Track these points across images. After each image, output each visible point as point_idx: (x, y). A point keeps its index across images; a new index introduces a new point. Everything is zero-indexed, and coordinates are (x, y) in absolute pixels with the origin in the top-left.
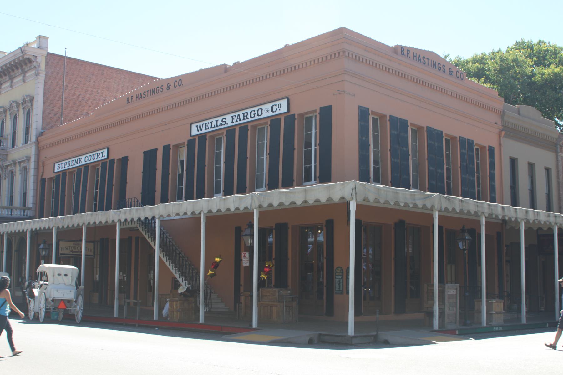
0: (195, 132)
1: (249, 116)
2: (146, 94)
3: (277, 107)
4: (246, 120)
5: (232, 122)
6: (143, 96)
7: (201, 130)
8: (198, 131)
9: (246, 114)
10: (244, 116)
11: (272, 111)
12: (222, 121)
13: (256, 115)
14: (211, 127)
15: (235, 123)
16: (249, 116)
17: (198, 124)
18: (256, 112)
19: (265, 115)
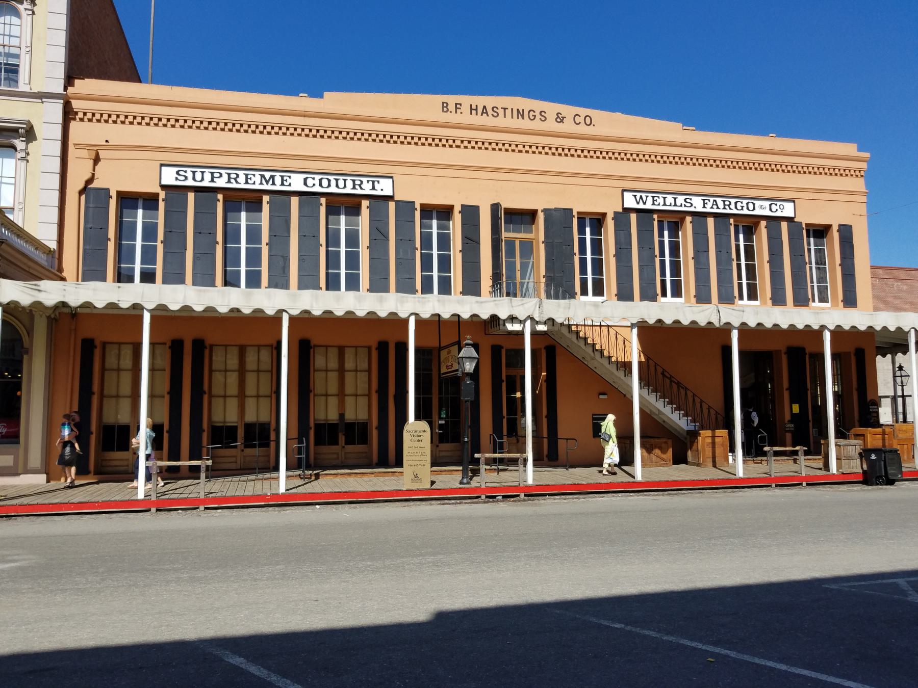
0: (630, 202)
1: (733, 206)
3: (778, 207)
4: (728, 211)
5: (704, 207)
7: (644, 203)
8: (638, 203)
9: (727, 203)
10: (725, 205)
11: (771, 210)
12: (685, 200)
13: (745, 208)
14: (665, 204)
15: (708, 210)
16: (733, 206)
17: (638, 195)
18: (744, 204)
19: (758, 212)
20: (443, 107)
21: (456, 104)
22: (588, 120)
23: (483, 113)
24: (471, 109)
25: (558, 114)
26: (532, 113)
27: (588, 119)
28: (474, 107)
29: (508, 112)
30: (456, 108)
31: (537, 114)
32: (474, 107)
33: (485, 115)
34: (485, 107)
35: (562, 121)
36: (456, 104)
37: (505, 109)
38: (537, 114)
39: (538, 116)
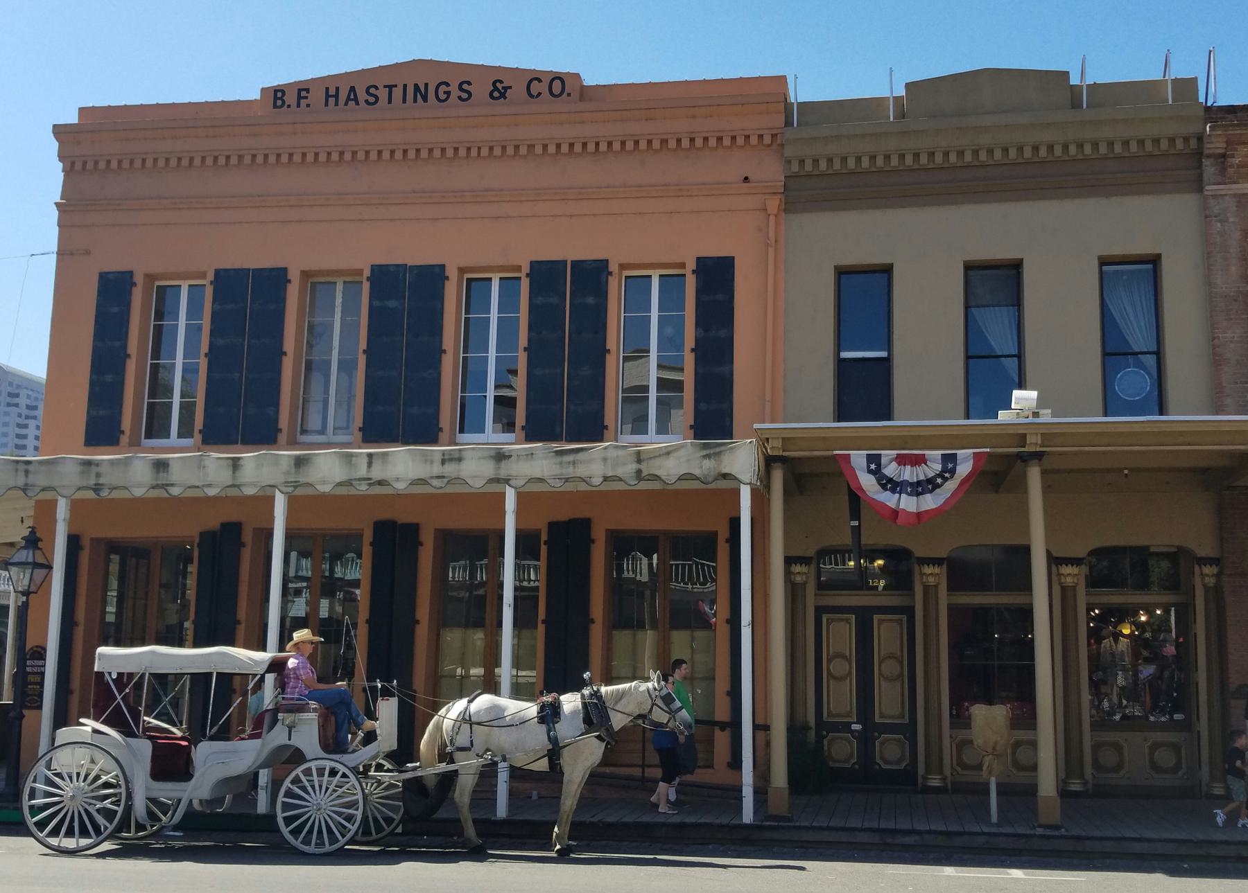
2: (383, 94)
6: (362, 96)
20: (276, 98)
21: (300, 91)
23: (348, 99)
24: (328, 96)
25: (494, 83)
26: (443, 88)
27: (557, 84)
29: (397, 93)
30: (300, 97)
31: (454, 89)
32: (332, 92)
33: (352, 103)
34: (352, 89)
35: (503, 96)
36: (300, 91)
37: (390, 87)
38: (454, 89)
39: (455, 92)
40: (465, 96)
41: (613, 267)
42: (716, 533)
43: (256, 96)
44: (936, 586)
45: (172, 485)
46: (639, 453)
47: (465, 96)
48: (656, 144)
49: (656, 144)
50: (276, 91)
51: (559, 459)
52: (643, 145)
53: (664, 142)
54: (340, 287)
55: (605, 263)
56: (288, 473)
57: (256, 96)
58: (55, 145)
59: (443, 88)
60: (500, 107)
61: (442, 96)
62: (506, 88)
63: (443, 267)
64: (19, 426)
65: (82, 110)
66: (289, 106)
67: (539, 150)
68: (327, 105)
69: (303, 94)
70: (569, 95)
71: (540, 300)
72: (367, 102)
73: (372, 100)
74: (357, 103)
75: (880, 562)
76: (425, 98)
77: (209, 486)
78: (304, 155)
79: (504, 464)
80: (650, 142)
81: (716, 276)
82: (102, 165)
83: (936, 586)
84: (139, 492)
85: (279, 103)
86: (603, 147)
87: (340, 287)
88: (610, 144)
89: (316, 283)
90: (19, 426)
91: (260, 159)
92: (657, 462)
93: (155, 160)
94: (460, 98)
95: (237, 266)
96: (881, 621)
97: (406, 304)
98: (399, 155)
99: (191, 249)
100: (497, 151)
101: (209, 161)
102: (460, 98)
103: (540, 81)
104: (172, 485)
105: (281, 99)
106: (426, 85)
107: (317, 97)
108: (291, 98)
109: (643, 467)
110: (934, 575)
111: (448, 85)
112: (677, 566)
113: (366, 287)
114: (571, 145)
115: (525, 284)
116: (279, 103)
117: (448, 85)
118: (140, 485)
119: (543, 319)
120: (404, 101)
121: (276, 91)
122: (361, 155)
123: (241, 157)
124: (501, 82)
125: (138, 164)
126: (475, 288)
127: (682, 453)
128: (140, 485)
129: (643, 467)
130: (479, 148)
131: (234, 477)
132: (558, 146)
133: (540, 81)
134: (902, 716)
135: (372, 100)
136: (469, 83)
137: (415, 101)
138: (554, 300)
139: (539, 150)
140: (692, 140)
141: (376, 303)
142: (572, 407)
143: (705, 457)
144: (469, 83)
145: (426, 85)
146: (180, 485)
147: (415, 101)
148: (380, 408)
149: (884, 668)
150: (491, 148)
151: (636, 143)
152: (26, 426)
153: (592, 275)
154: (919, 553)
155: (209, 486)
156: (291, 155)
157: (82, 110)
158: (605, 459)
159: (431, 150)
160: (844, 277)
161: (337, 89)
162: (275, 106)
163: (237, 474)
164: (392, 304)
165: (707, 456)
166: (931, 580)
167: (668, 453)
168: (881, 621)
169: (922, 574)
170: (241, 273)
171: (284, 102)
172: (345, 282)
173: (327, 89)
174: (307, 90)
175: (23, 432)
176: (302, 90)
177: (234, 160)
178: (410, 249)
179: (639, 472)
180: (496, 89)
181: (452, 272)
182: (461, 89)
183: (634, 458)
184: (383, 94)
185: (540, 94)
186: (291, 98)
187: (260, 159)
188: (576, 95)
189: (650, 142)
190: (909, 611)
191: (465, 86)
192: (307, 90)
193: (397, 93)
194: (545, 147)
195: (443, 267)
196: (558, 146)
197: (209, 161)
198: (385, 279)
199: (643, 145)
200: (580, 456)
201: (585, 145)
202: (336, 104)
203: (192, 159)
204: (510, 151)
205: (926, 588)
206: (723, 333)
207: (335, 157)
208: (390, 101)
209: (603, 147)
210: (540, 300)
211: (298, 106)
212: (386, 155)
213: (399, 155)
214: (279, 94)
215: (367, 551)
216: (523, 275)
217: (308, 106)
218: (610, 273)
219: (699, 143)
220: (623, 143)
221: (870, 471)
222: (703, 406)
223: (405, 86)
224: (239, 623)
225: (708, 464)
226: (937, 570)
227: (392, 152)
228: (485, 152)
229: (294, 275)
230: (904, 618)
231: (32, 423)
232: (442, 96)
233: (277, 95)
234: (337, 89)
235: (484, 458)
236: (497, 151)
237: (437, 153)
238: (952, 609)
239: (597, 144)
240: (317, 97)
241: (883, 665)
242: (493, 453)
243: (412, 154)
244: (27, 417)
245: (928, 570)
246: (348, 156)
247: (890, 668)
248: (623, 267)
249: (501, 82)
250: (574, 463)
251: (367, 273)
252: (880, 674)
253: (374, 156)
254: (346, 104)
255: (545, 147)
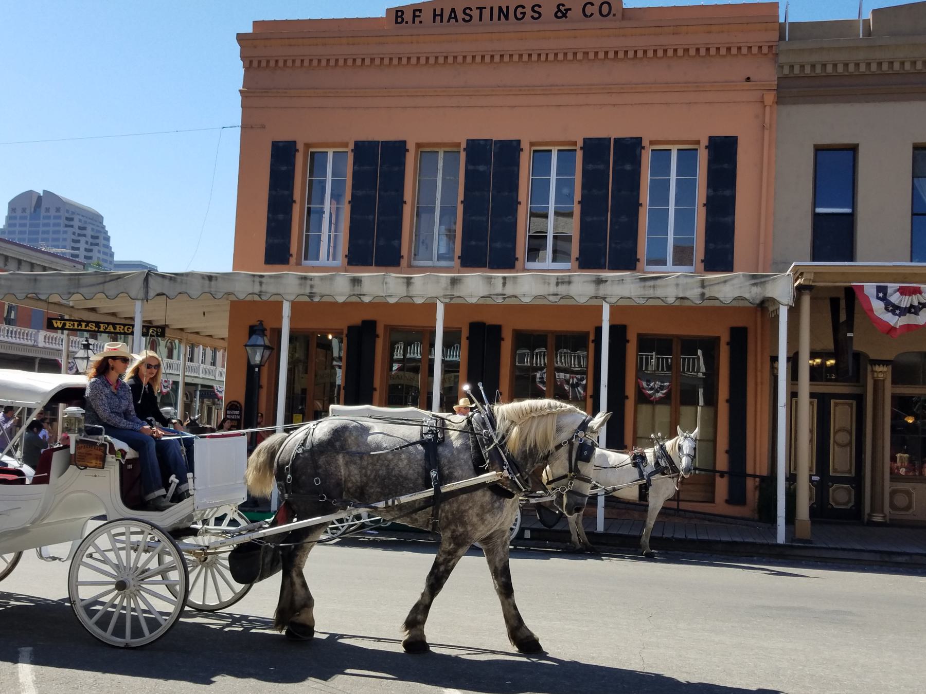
2: (475, 14)
6: (460, 15)
20: (397, 17)
21: (414, 11)
22: (605, 9)
23: (450, 18)
24: (435, 15)
26: (520, 10)
28: (439, 12)
29: (487, 13)
30: (414, 16)
31: (528, 11)
32: (439, 12)
33: (453, 21)
34: (453, 10)
35: (565, 15)
36: (414, 11)
37: (481, 9)
38: (528, 11)
39: (529, 13)
40: (536, 15)
41: (645, 143)
42: (718, 338)
43: (383, 14)
44: (884, 381)
45: (364, 295)
46: (703, 281)
47: (536, 15)
48: (680, 52)
49: (680, 52)
50: (397, 12)
51: (643, 284)
52: (670, 53)
53: (687, 50)
54: (441, 156)
55: (639, 140)
56: (446, 289)
57: (383, 14)
58: (238, 48)
59: (520, 10)
60: (562, 24)
61: (520, 16)
62: (567, 10)
63: (519, 142)
64: (74, 241)
65: (255, 23)
66: (407, 23)
67: (591, 56)
68: (434, 22)
69: (417, 13)
70: (614, 15)
71: (590, 167)
72: (464, 20)
73: (467, 18)
74: (457, 21)
75: (832, 362)
76: (507, 18)
77: (390, 296)
78: (418, 58)
79: (602, 286)
80: (675, 50)
81: (723, 151)
82: (272, 64)
83: (884, 381)
84: (341, 299)
85: (400, 20)
86: (640, 54)
87: (441, 156)
88: (645, 52)
89: (427, 151)
90: (74, 241)
91: (386, 61)
92: (716, 288)
93: (311, 61)
94: (532, 17)
95: (370, 139)
96: (836, 405)
97: (492, 168)
98: (488, 59)
99: (334, 128)
100: (561, 57)
101: (350, 62)
102: (532, 17)
103: (592, 4)
104: (364, 295)
105: (401, 17)
106: (508, 7)
107: (427, 16)
108: (408, 16)
109: (706, 291)
110: (883, 372)
111: (523, 7)
112: (684, 359)
113: (463, 155)
114: (616, 53)
115: (579, 155)
116: (400, 20)
117: (523, 7)
118: (341, 295)
119: (592, 180)
120: (491, 19)
121: (397, 12)
122: (460, 59)
123: (372, 60)
124: (563, 5)
125: (298, 63)
126: (541, 156)
127: (735, 281)
128: (341, 295)
129: (706, 291)
130: (547, 55)
131: (408, 291)
132: (606, 53)
133: (592, 4)
134: (850, 471)
135: (467, 18)
136: (539, 6)
137: (499, 19)
138: (601, 167)
139: (591, 56)
140: (708, 49)
141: (471, 167)
142: (613, 245)
143: (753, 285)
144: (539, 6)
145: (508, 7)
146: (370, 295)
147: (499, 19)
148: (473, 243)
149: (839, 438)
150: (556, 55)
151: (665, 51)
152: (78, 241)
153: (629, 149)
154: (873, 356)
155: (390, 296)
156: (409, 59)
157: (255, 23)
158: (677, 285)
159: (511, 56)
160: (819, 152)
161: (442, 10)
162: (397, 22)
163: (411, 288)
164: (482, 168)
165: (755, 284)
166: (881, 376)
167: (725, 282)
168: (836, 405)
169: (873, 371)
170: (373, 144)
171: (403, 19)
172: (445, 152)
173: (435, 10)
174: (420, 11)
175: (77, 245)
176: (416, 11)
177: (368, 62)
178: (495, 128)
179: (703, 294)
180: (559, 10)
181: (525, 145)
182: (533, 10)
183: (699, 284)
184: (475, 14)
185: (592, 14)
186: (408, 16)
187: (386, 61)
188: (619, 15)
189: (675, 50)
190: (860, 399)
191: (536, 9)
192: (420, 11)
193: (487, 13)
194: (596, 53)
195: (519, 142)
196: (606, 53)
197: (350, 62)
198: (477, 150)
199: (670, 53)
200: (659, 282)
201: (626, 52)
202: (441, 21)
203: (337, 60)
204: (570, 57)
205: (876, 382)
206: (728, 193)
207: (441, 60)
208: (481, 19)
209: (640, 54)
210: (590, 167)
211: (414, 22)
212: (478, 59)
213: (488, 59)
214: (400, 14)
215: (465, 343)
216: (578, 148)
217: (421, 22)
218: (643, 148)
219: (713, 51)
220: (655, 51)
221: (878, 298)
222: (712, 246)
223: (492, 8)
224: (375, 389)
225: (756, 290)
226: (885, 369)
227: (483, 57)
228: (551, 57)
229: (411, 146)
230: (854, 403)
231: (83, 239)
232: (520, 16)
233: (398, 14)
234: (442, 10)
235: (587, 282)
236: (561, 57)
237: (516, 58)
238: (894, 397)
239: (636, 52)
240: (427, 16)
241: (837, 437)
242: (594, 279)
243: (497, 58)
244: (79, 235)
245: (878, 368)
246: (450, 60)
247: (843, 438)
248: (652, 143)
249: (563, 5)
250: (654, 287)
251: (464, 145)
252: (834, 441)
253: (469, 59)
254: (448, 21)
255: (596, 53)
